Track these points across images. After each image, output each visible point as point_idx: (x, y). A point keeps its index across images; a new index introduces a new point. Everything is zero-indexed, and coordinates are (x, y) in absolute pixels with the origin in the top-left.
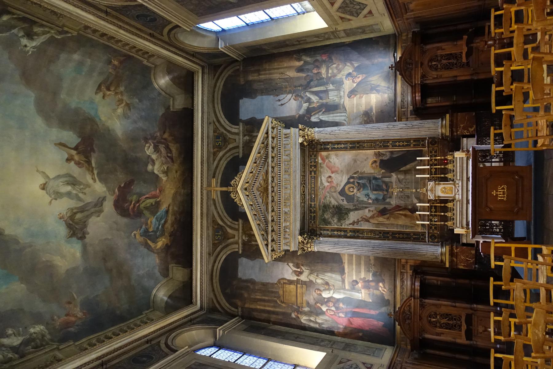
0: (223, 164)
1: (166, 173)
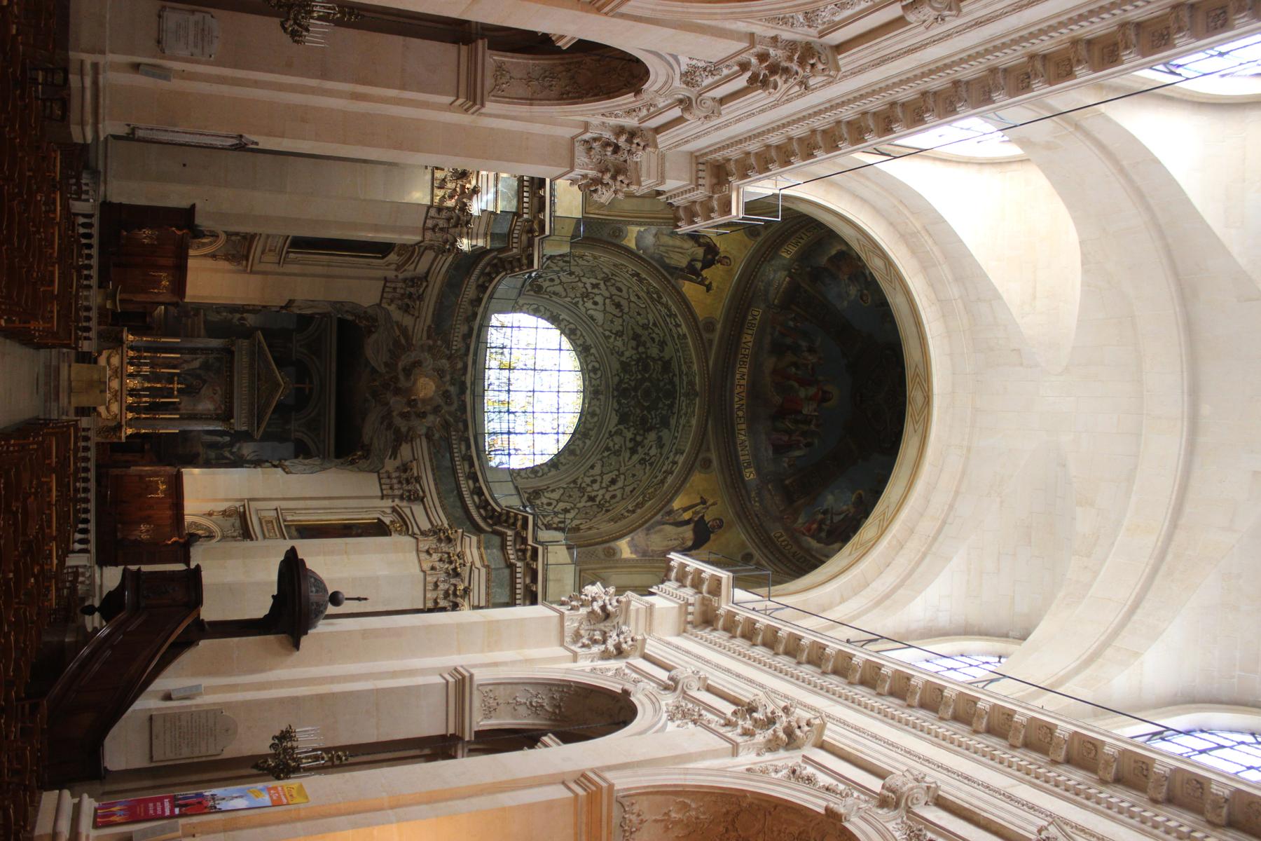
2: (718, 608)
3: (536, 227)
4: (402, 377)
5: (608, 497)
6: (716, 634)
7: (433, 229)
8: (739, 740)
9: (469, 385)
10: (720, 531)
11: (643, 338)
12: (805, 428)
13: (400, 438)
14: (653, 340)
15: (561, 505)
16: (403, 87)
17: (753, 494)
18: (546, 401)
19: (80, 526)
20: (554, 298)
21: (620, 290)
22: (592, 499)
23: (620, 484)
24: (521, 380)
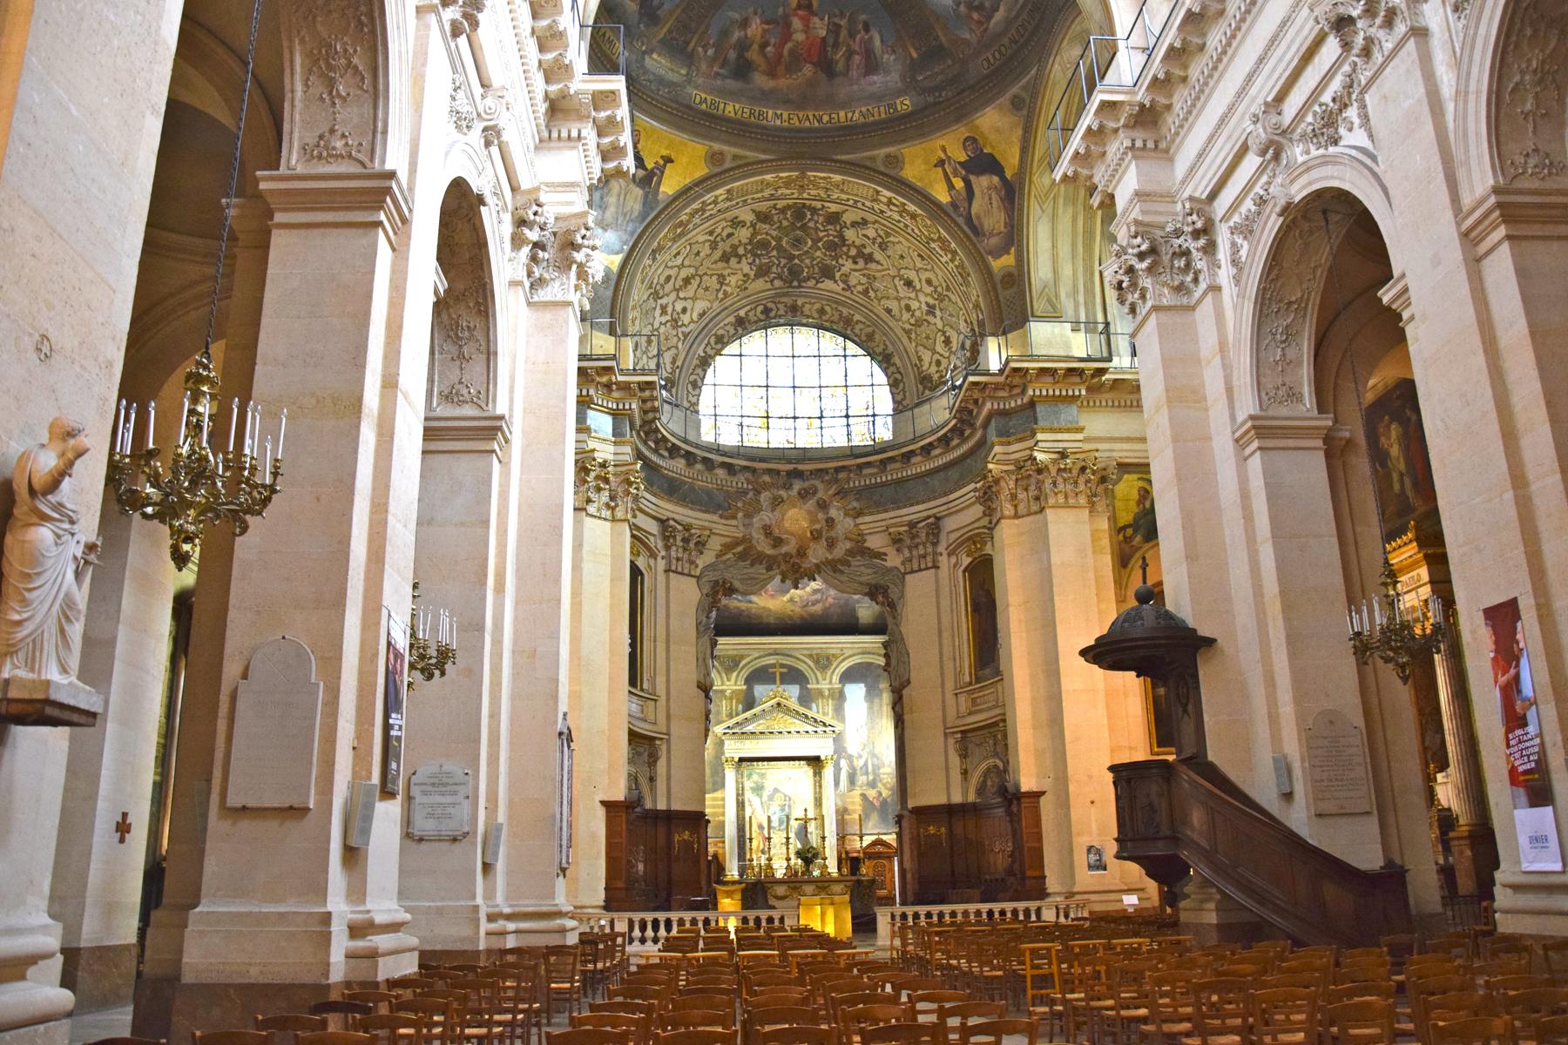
0: (802, 667)
1: (791, 600)
2: (1142, 106)
3: (604, 379)
4: (784, 550)
5: (929, 290)
6: (1177, 108)
7: (613, 509)
8: (1401, 28)
9: (791, 467)
10: (980, 141)
11: (728, 250)
12: (844, 33)
13: (860, 549)
14: (730, 235)
15: (939, 347)
16: (486, 523)
17: (930, 99)
18: (806, 372)
19: (1021, 917)
20: (679, 363)
21: (668, 278)
22: (931, 310)
23: (912, 275)
24: (781, 403)
